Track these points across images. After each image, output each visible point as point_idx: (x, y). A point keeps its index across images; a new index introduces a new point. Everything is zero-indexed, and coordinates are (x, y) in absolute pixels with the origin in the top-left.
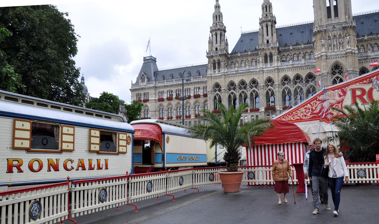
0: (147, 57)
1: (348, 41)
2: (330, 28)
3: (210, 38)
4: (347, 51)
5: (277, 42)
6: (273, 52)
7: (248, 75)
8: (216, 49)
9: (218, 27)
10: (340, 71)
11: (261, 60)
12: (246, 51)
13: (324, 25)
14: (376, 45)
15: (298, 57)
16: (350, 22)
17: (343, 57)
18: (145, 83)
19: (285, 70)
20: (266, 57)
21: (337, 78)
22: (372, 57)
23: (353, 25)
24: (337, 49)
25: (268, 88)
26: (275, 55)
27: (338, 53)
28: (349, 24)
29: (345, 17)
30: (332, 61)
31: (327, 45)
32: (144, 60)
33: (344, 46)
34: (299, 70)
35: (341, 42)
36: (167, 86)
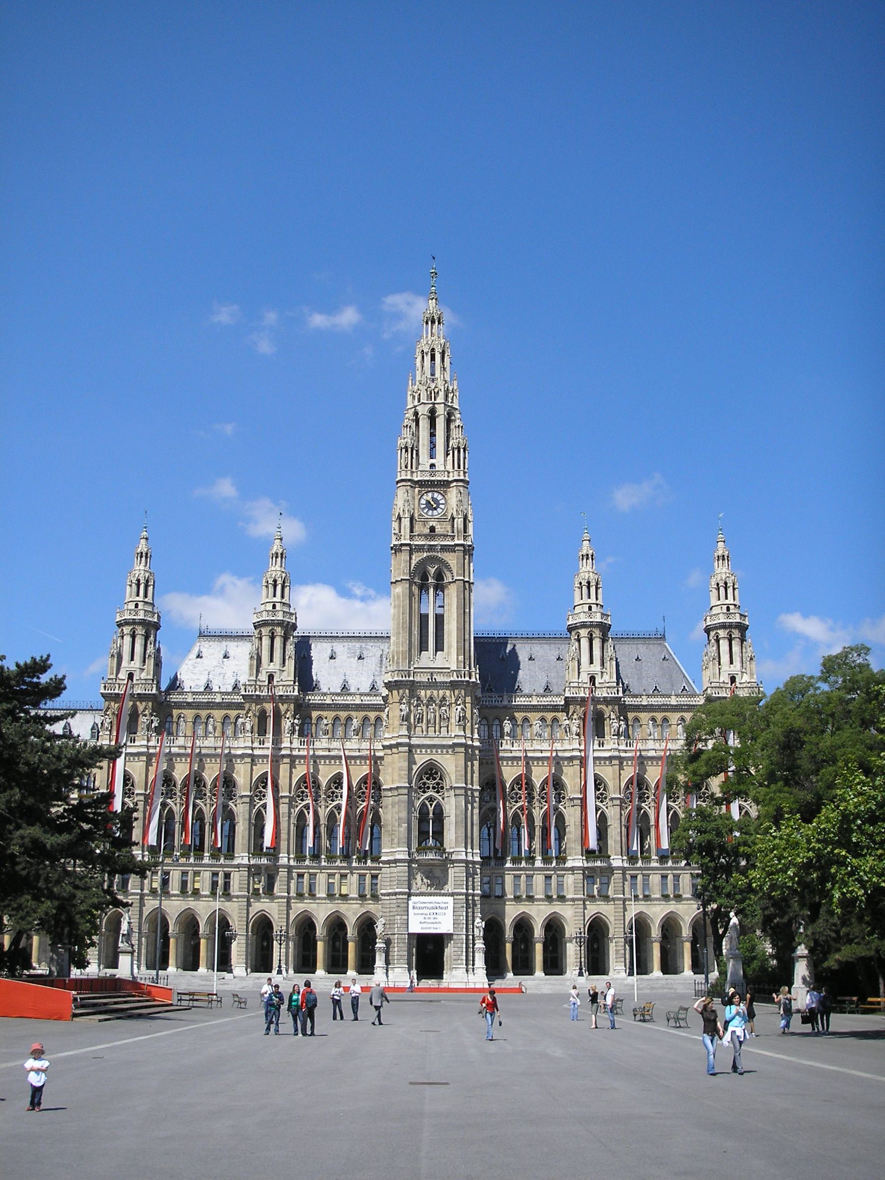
1: (460, 717)
4: (456, 741)
8: (131, 676)
10: (438, 784)
21: (431, 799)
23: (473, 680)
24: (435, 732)
26: (288, 718)
29: (458, 659)
30: (421, 759)
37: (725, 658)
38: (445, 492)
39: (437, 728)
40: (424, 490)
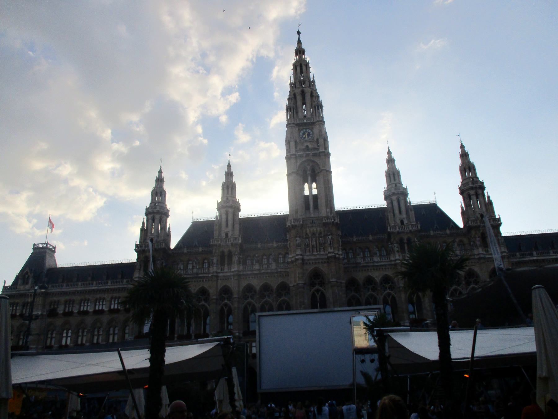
0: (39, 244)
1: (330, 242)
3: (143, 223)
5: (239, 237)
7: (195, 281)
9: (158, 209)
11: (215, 261)
13: (300, 219)
14: (367, 250)
15: (268, 259)
16: (332, 217)
17: (325, 262)
18: (27, 287)
19: (249, 278)
21: (318, 291)
22: (362, 265)
23: (336, 221)
24: (317, 252)
25: (224, 302)
26: (236, 255)
27: (318, 257)
28: (331, 220)
29: (326, 211)
31: (304, 246)
32: (34, 249)
33: (325, 248)
34: (267, 277)
35: (322, 243)
36: (66, 293)
38: (313, 128)
39: (318, 249)
40: (301, 128)
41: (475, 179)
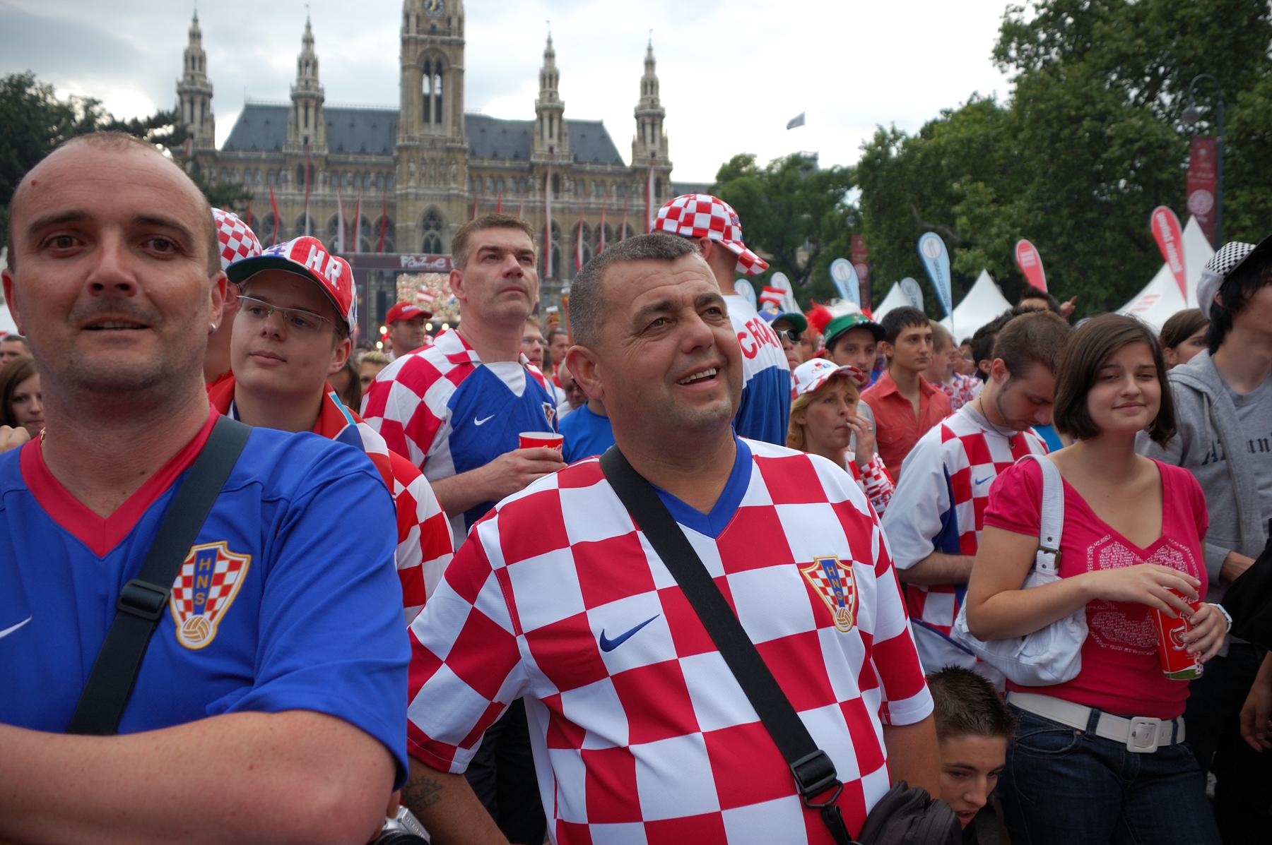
2: (427, 145)
4: (451, 192)
6: (315, 163)
11: (290, 177)
12: (255, 148)
20: (300, 170)
21: (432, 236)
24: (435, 184)
37: (649, 138)
41: (654, 103)
